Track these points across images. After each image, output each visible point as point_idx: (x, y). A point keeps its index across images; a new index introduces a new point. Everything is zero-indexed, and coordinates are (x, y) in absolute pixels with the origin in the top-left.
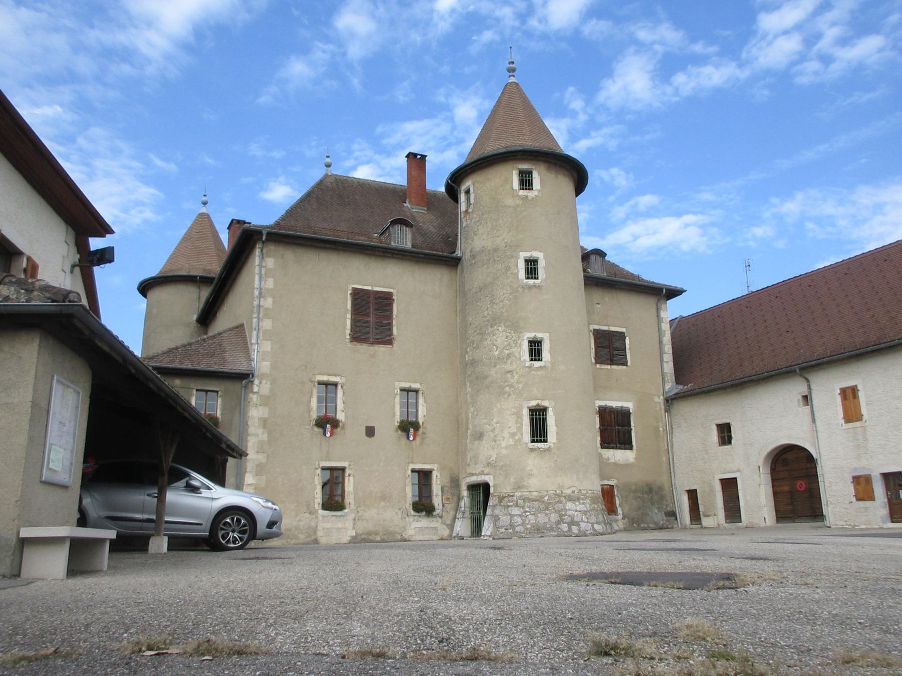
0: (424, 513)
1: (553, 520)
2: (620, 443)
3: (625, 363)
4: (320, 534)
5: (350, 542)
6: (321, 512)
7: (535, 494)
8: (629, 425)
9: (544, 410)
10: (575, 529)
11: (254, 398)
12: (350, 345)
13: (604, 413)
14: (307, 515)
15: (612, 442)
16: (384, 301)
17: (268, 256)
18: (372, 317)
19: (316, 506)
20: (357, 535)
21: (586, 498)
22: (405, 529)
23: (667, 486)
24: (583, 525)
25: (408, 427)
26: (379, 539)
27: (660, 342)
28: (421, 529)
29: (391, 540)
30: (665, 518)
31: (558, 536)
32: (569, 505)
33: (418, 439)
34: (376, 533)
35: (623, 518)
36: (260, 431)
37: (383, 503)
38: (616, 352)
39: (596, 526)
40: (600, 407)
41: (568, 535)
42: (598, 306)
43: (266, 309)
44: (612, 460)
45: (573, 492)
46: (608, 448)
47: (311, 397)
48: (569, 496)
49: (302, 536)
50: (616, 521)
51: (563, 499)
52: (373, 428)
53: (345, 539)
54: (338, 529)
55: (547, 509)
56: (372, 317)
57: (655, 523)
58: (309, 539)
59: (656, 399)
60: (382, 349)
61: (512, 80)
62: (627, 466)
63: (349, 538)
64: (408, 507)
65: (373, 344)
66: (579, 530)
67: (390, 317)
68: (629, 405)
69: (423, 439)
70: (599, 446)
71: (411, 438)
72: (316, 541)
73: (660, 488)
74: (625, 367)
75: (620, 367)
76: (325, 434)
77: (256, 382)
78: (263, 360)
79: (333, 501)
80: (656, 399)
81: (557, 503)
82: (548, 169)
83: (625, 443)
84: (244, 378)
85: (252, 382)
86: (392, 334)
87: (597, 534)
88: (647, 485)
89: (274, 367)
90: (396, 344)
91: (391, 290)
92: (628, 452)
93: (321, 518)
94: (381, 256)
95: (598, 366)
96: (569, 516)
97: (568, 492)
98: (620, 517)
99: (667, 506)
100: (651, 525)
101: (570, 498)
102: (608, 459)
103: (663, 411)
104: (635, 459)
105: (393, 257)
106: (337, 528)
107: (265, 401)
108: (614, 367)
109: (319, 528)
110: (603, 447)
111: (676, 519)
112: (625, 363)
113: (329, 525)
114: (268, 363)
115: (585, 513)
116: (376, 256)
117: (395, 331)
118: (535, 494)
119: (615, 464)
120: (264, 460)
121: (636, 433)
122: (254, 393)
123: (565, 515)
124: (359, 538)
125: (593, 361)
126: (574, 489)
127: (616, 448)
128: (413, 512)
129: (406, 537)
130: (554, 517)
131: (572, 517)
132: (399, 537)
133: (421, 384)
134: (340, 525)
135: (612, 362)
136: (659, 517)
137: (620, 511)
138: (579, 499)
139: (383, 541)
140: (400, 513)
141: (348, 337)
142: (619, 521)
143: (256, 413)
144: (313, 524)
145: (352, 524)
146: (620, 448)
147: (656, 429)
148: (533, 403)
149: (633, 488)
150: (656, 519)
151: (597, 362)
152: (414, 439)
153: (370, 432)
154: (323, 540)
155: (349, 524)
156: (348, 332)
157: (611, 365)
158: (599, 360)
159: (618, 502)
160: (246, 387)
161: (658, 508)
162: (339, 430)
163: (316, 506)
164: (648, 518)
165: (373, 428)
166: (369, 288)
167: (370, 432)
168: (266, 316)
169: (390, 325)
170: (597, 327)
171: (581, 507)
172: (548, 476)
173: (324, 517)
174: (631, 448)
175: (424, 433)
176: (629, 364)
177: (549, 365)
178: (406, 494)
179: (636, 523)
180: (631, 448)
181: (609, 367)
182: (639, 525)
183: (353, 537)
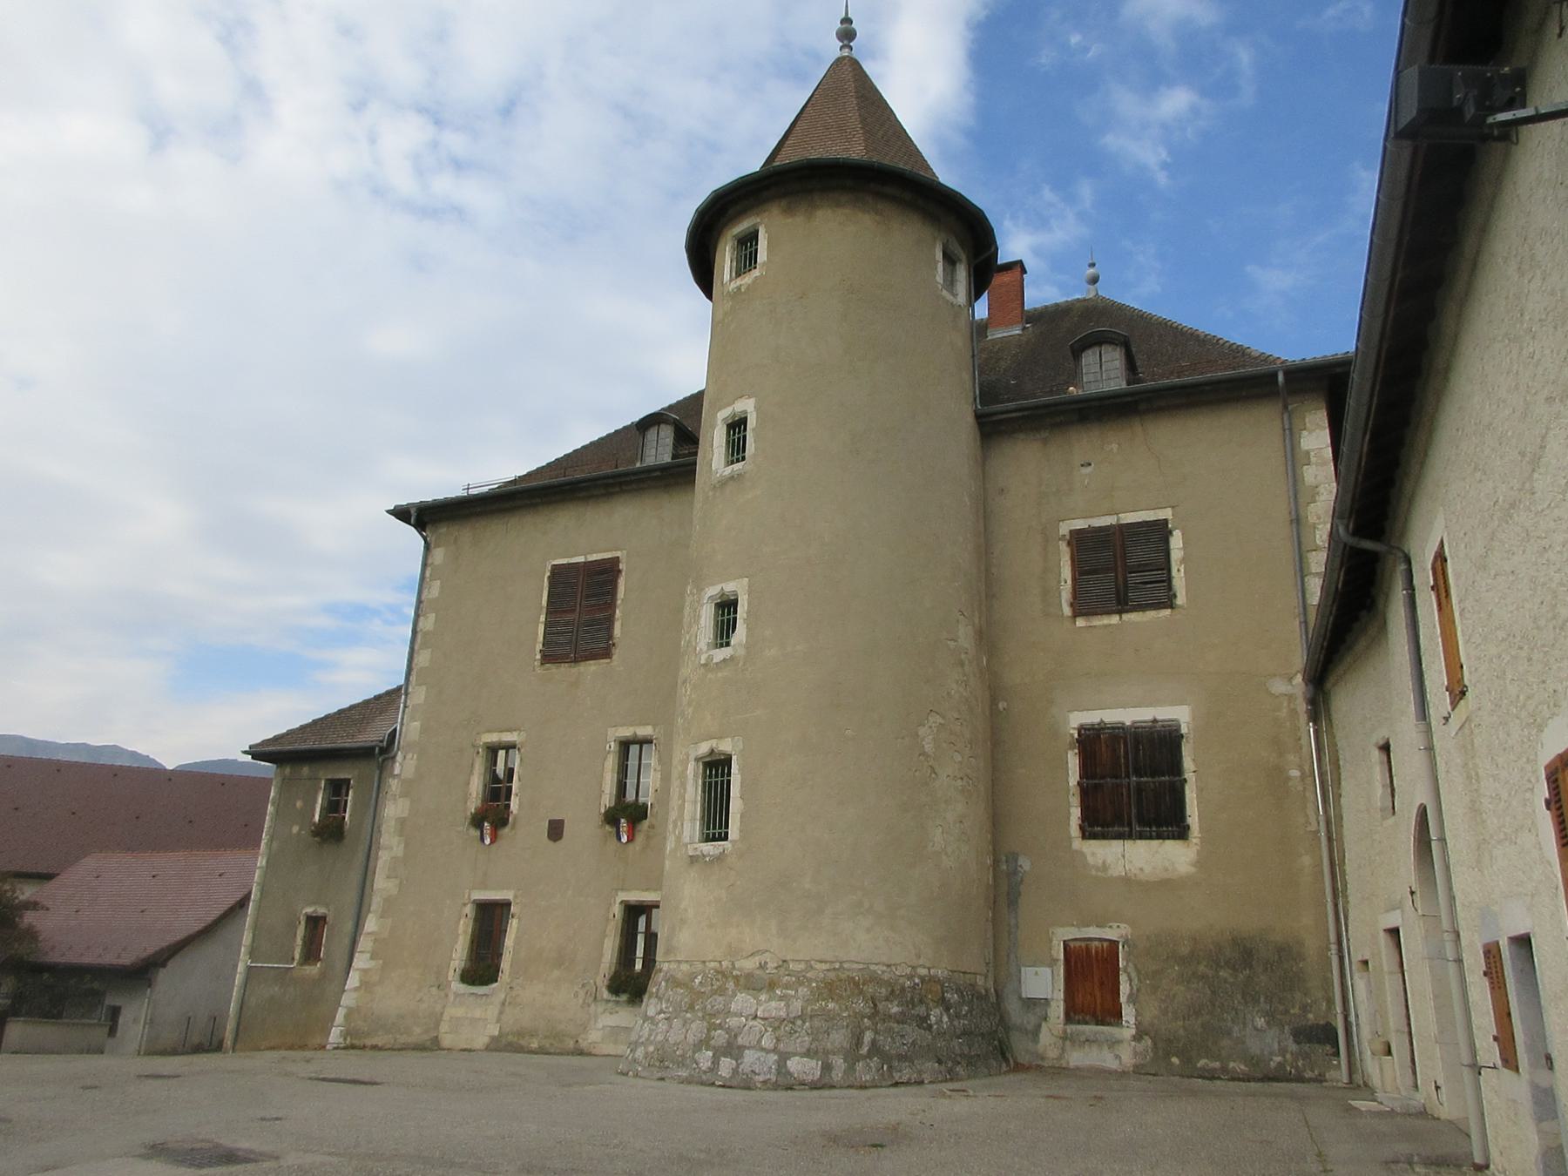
0: (624, 997)
1: (691, 1038)
2: (1141, 822)
3: (1169, 602)
4: (444, 1027)
5: (488, 1048)
6: (457, 986)
7: (685, 967)
8: (1176, 767)
9: (726, 762)
10: (726, 1064)
11: (393, 785)
12: (539, 671)
13: (1091, 742)
14: (434, 990)
15: (1118, 819)
16: (602, 577)
17: (437, 546)
18: (582, 611)
19: (451, 972)
20: (501, 1035)
21: (801, 980)
22: (585, 1028)
23: (1311, 945)
24: (750, 1056)
25: (627, 814)
26: (535, 1045)
27: (1297, 521)
28: (615, 1032)
29: (564, 1047)
30: (1293, 1047)
31: (688, 1081)
32: (742, 1001)
33: (640, 838)
34: (533, 1034)
35: (1138, 1037)
36: (395, 840)
37: (556, 973)
38: (1134, 578)
39: (794, 1065)
40: (1081, 729)
41: (707, 1081)
42: (1089, 469)
43: (426, 634)
44: (1117, 871)
45: (762, 966)
46: (1104, 836)
47: (471, 773)
48: (749, 976)
49: (418, 1030)
50: (1114, 1043)
51: (731, 985)
52: (561, 822)
53: (481, 1041)
54: (474, 1021)
55: (691, 1007)
56: (582, 611)
57: (1253, 1061)
58: (426, 1037)
59: (1279, 687)
60: (591, 668)
61: (846, 52)
62: (1167, 885)
63: (486, 1040)
64: (599, 983)
65: (576, 661)
66: (735, 1071)
67: (611, 605)
68: (1180, 714)
69: (648, 837)
70: (1075, 831)
71: (624, 839)
72: (436, 1040)
73: (1287, 953)
74: (1168, 612)
75: (1151, 614)
76: (482, 839)
77: (399, 757)
78: (413, 719)
79: (482, 967)
80: (1279, 687)
81: (714, 992)
82: (789, 211)
83: (1163, 817)
84: (380, 754)
85: (394, 757)
86: (611, 637)
87: (785, 1083)
88: (1235, 942)
89: (424, 730)
90: (617, 653)
91: (618, 554)
92: (1171, 847)
93: (451, 997)
94: (603, 495)
95: (1080, 622)
96: (728, 1030)
97: (749, 965)
98: (1127, 1030)
99: (1305, 1008)
100: (1238, 1066)
101: (750, 983)
102: (1105, 867)
103: (1303, 717)
104: (1199, 863)
105: (623, 492)
106: (474, 1017)
107: (408, 788)
108: (1125, 617)
109: (446, 1017)
110: (1087, 835)
111: (1337, 1054)
112: (1169, 602)
113: (459, 1012)
114: (417, 724)
115: (776, 1023)
116: (597, 496)
117: (617, 631)
118: (685, 967)
119: (1127, 881)
120: (395, 891)
121: (1200, 791)
122: (394, 776)
123: (720, 1026)
124: (504, 1041)
125: (1067, 611)
126: (767, 957)
127: (1130, 836)
128: (606, 994)
129: (583, 1044)
130: (697, 1029)
131: (733, 1034)
132: (571, 1044)
133: (654, 726)
134: (478, 1013)
135: (1122, 604)
136: (1265, 1039)
137: (1128, 1013)
138: (771, 986)
139: (542, 1051)
140: (582, 994)
141: (538, 657)
142: (1118, 1047)
143: (393, 810)
144: (438, 1008)
145: (496, 1012)
146: (1141, 837)
147: (1277, 775)
148: (704, 748)
149: (1185, 950)
150: (1254, 1046)
151: (1076, 615)
152: (630, 840)
153: (556, 830)
154: (447, 1041)
155: (492, 1012)
156: (539, 646)
157: (1120, 612)
158: (1084, 605)
159: (1124, 989)
160: (381, 769)
161: (1271, 1017)
162: (506, 830)
163: (451, 972)
164: (1225, 1042)
165: (561, 822)
166: (581, 559)
167: (556, 830)
168: (424, 645)
169: (610, 621)
170: (1080, 524)
171: (775, 1008)
172: (711, 926)
173: (457, 995)
174: (1182, 833)
175: (652, 827)
176: (1181, 600)
177: (741, 652)
178: (601, 955)
179: (1181, 1058)
180: (1182, 833)
181: (1115, 619)
182: (1188, 1061)
183: (493, 1039)
